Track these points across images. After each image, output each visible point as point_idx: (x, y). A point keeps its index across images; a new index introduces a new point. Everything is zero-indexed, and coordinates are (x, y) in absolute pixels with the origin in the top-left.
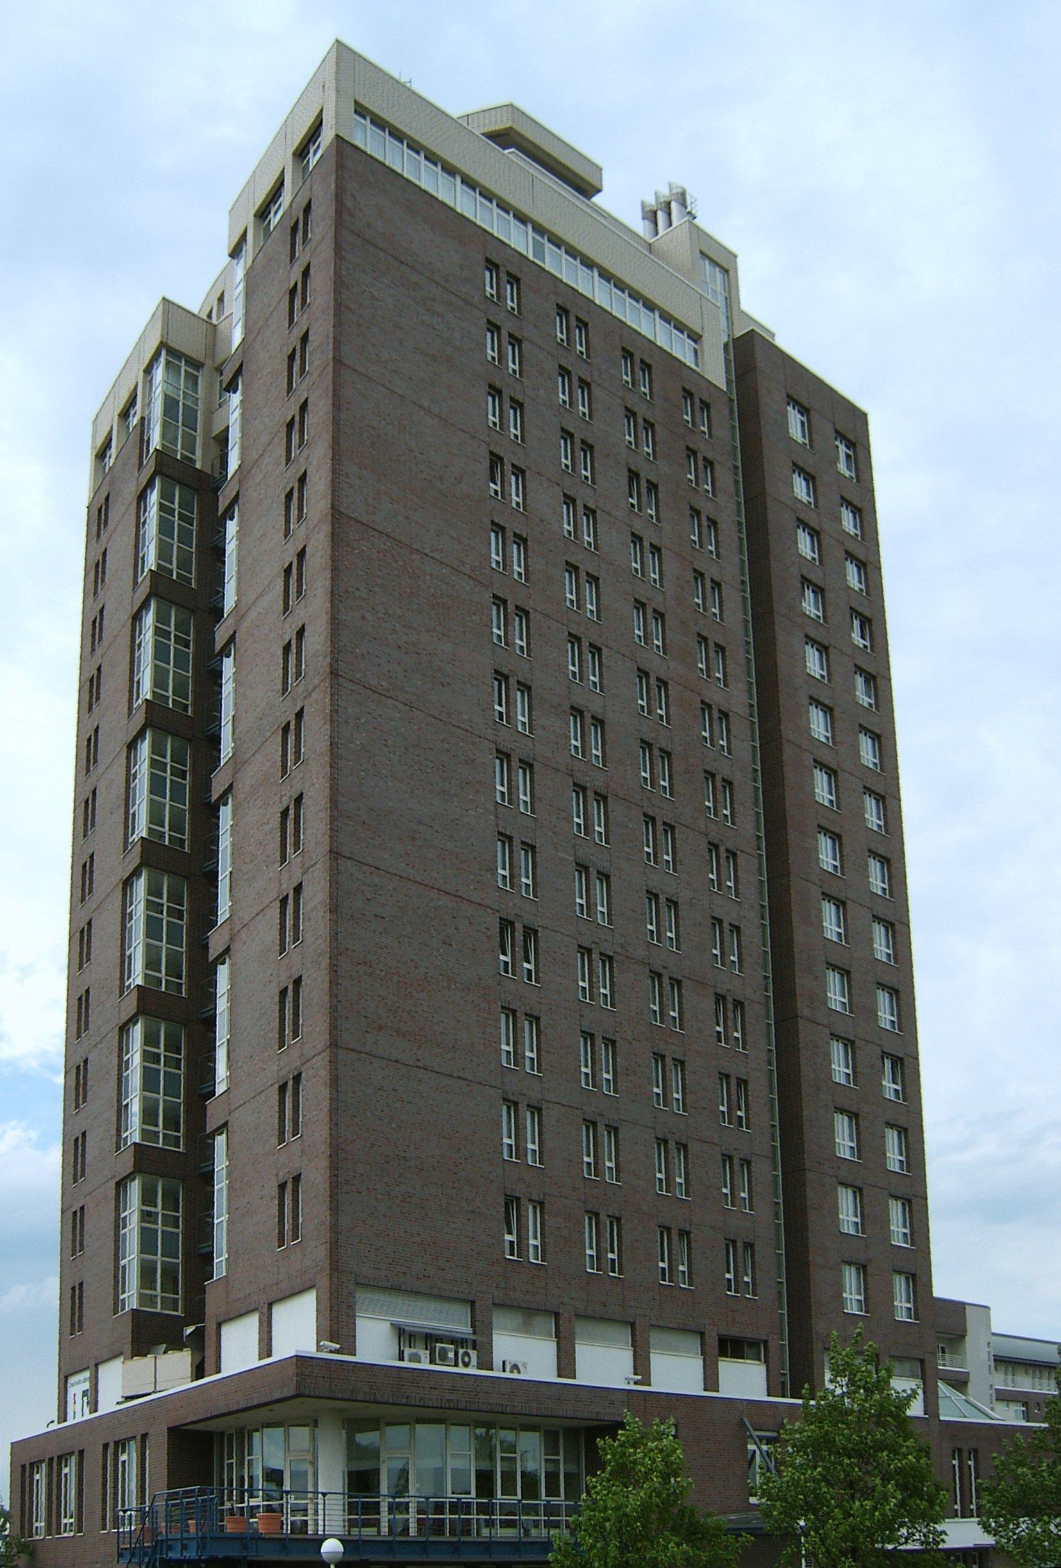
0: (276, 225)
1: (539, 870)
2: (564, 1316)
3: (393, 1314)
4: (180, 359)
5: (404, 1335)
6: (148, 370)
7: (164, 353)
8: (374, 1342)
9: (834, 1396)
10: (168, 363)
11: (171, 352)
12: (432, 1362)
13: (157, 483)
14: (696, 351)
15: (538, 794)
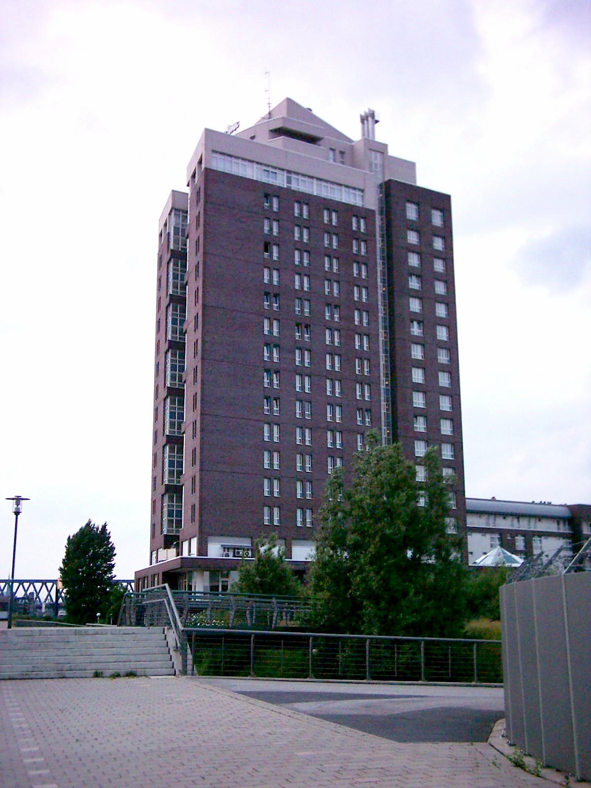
0: (169, 548)
1: (281, 404)
2: (288, 539)
3: (221, 542)
4: (179, 212)
5: (225, 548)
6: (170, 214)
7: (173, 211)
8: (215, 550)
9: (322, 616)
10: (175, 214)
11: (176, 210)
12: (234, 556)
13: (172, 260)
14: (362, 196)
15: (281, 381)
